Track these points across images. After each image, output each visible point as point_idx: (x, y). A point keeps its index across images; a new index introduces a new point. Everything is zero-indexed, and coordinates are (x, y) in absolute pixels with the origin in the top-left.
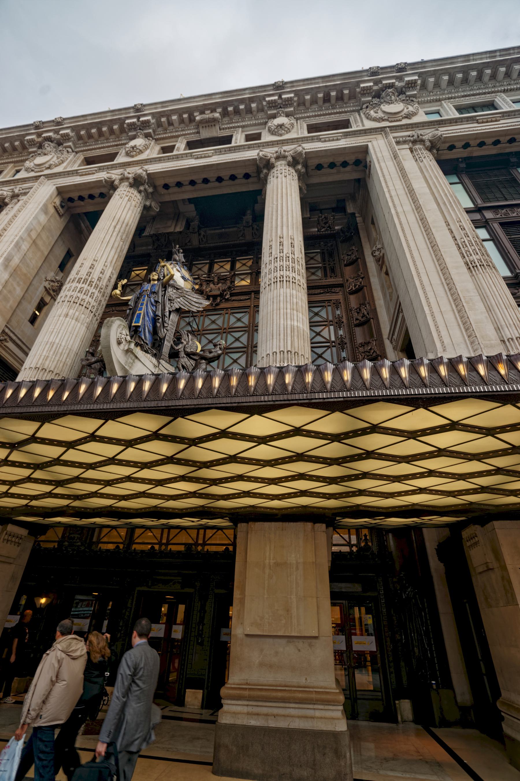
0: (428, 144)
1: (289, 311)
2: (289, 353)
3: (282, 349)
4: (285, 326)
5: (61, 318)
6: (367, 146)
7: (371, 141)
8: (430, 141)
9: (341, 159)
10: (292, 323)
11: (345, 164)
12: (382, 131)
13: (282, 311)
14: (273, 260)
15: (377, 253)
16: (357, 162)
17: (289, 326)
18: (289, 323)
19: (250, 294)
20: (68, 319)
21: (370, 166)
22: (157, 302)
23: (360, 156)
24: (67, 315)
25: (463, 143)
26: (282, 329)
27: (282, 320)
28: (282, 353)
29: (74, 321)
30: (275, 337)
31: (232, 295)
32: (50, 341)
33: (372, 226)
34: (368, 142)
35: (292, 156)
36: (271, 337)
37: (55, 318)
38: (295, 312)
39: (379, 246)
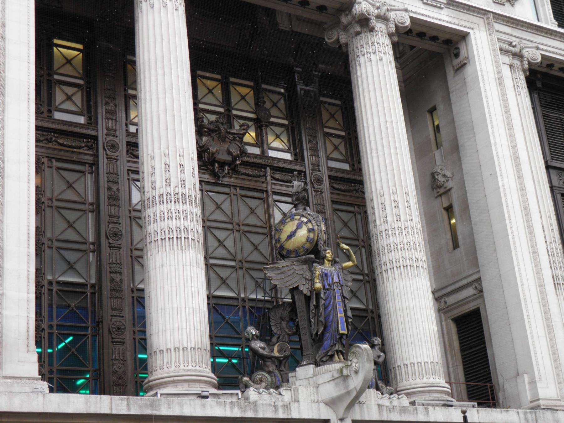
0: (526, 66)
6: (468, 34)
7: (473, 29)
8: (529, 61)
9: (435, 34)
11: (434, 39)
12: (484, 14)
15: (441, 179)
16: (448, 42)
19: (265, 168)
21: (465, 64)
23: (454, 38)
25: (550, 63)
31: (244, 163)
33: (428, 116)
34: (470, 28)
35: (396, 25)
39: (448, 174)
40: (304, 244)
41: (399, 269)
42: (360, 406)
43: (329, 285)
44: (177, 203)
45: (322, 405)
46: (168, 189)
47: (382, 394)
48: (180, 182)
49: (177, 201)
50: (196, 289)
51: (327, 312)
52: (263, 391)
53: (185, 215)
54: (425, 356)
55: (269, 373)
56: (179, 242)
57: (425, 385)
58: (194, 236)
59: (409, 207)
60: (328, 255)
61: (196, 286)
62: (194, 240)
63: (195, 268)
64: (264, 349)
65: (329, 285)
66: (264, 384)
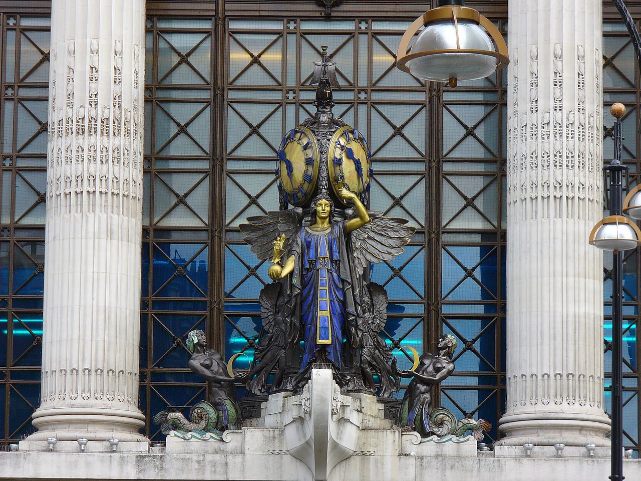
1: (571, 279)
2: (571, 376)
3: (559, 371)
4: (565, 319)
5: (103, 242)
10: (577, 311)
13: (559, 279)
14: (540, 129)
17: (571, 319)
18: (571, 310)
20: (115, 242)
22: (343, 281)
24: (110, 234)
26: (559, 325)
27: (559, 303)
28: (558, 377)
29: (125, 243)
30: (546, 341)
32: (102, 304)
36: (539, 341)
37: (91, 242)
38: (582, 279)
40: (302, 185)
41: (546, 200)
42: (362, 459)
43: (311, 262)
44: (80, 136)
45: (287, 458)
46: (70, 111)
47: (425, 434)
48: (88, 98)
49: (81, 132)
50: (102, 276)
51: (305, 307)
52: (192, 436)
53: (92, 153)
54: (546, 362)
55: (216, 406)
56: (79, 199)
57: (533, 416)
58: (107, 187)
59: (558, 84)
60: (319, 209)
61: (103, 269)
62: (106, 193)
63: (103, 242)
64: (208, 367)
65: (311, 262)
66: (203, 424)
